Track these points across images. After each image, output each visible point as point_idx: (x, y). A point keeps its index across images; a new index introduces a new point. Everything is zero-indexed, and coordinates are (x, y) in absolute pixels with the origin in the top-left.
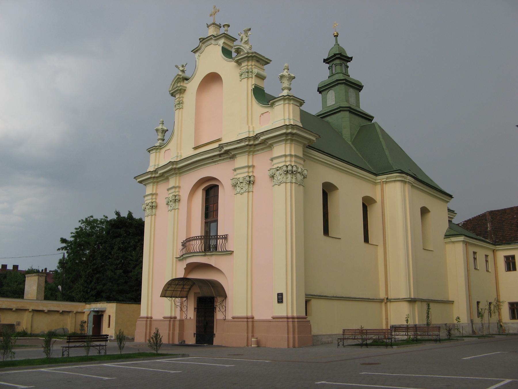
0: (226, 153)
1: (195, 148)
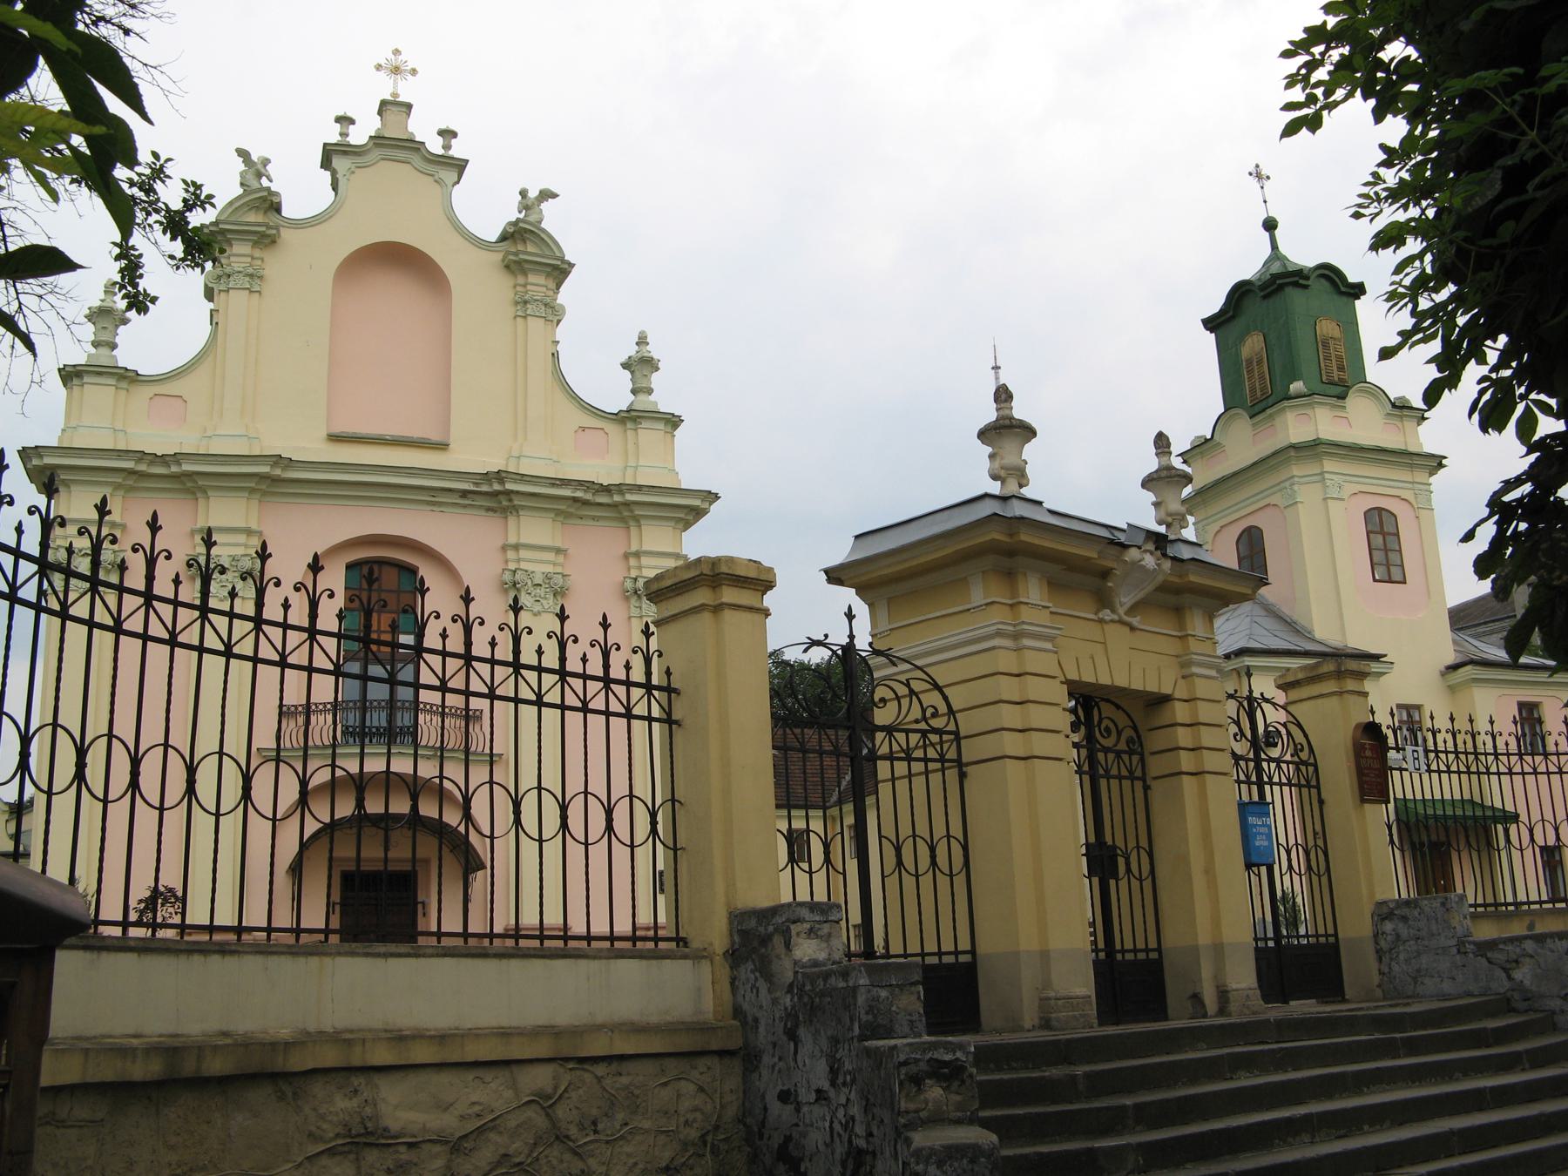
0: (496, 495)
1: (335, 438)
